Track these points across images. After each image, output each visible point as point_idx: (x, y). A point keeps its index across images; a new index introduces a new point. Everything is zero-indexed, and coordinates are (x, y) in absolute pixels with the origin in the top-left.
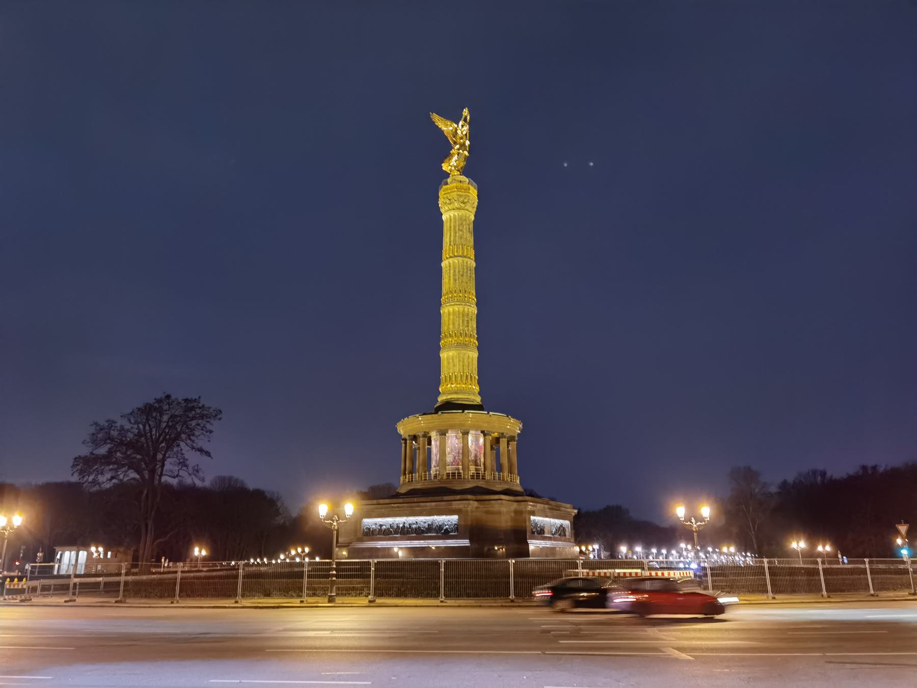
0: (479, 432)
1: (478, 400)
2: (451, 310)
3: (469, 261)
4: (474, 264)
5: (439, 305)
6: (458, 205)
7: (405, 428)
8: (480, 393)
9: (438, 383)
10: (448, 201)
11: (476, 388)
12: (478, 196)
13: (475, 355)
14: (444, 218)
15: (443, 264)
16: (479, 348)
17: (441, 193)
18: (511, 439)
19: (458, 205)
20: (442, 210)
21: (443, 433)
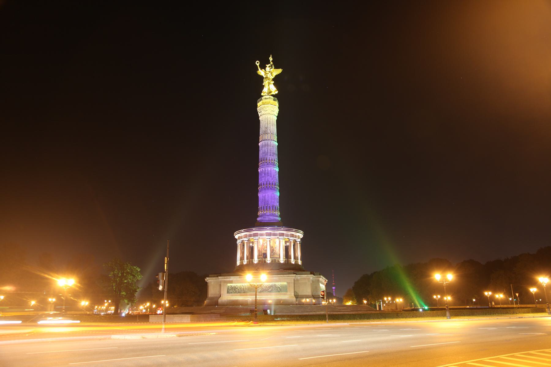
4: (277, 144)
6: (268, 110)
8: (280, 216)
9: (257, 210)
11: (278, 213)
14: (260, 119)
15: (260, 144)
19: (268, 110)
20: (259, 114)
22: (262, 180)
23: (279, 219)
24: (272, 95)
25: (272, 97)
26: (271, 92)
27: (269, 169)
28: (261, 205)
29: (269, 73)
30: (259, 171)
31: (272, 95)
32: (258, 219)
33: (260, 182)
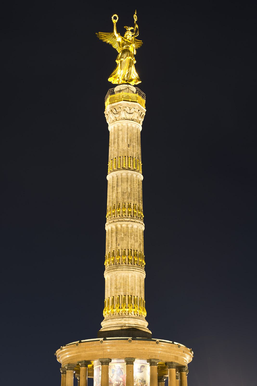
0: (145, 362)
1: (143, 324)
2: (114, 227)
3: (135, 174)
4: (142, 178)
5: (104, 221)
7: (65, 354)
9: (102, 306)
10: (114, 111)
12: (146, 105)
13: (144, 275)
14: (110, 128)
15: (109, 177)
16: (147, 269)
17: (107, 103)
18: (180, 368)
21: (105, 362)
22: (111, 246)
23: (146, 324)
24: (135, 86)
25: (134, 89)
26: (131, 80)
27: (124, 224)
28: (108, 295)
29: (124, 42)
30: (107, 229)
31: (135, 86)
32: (103, 324)
33: (108, 251)
